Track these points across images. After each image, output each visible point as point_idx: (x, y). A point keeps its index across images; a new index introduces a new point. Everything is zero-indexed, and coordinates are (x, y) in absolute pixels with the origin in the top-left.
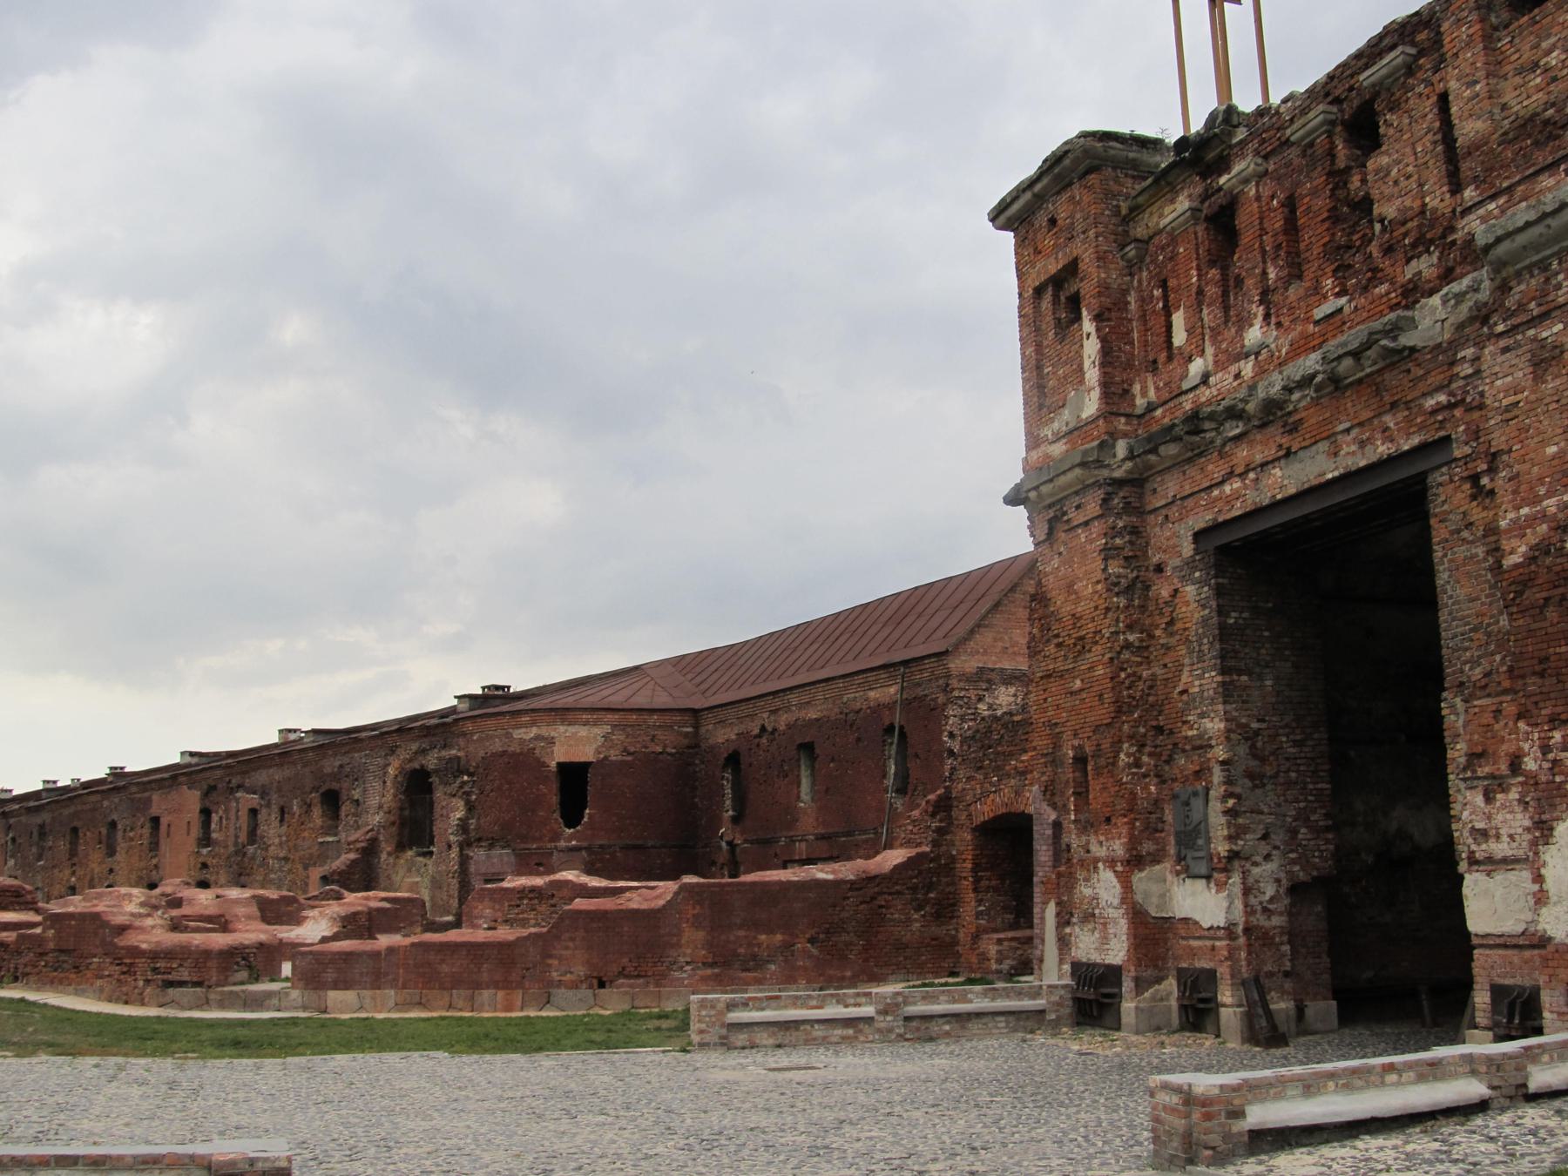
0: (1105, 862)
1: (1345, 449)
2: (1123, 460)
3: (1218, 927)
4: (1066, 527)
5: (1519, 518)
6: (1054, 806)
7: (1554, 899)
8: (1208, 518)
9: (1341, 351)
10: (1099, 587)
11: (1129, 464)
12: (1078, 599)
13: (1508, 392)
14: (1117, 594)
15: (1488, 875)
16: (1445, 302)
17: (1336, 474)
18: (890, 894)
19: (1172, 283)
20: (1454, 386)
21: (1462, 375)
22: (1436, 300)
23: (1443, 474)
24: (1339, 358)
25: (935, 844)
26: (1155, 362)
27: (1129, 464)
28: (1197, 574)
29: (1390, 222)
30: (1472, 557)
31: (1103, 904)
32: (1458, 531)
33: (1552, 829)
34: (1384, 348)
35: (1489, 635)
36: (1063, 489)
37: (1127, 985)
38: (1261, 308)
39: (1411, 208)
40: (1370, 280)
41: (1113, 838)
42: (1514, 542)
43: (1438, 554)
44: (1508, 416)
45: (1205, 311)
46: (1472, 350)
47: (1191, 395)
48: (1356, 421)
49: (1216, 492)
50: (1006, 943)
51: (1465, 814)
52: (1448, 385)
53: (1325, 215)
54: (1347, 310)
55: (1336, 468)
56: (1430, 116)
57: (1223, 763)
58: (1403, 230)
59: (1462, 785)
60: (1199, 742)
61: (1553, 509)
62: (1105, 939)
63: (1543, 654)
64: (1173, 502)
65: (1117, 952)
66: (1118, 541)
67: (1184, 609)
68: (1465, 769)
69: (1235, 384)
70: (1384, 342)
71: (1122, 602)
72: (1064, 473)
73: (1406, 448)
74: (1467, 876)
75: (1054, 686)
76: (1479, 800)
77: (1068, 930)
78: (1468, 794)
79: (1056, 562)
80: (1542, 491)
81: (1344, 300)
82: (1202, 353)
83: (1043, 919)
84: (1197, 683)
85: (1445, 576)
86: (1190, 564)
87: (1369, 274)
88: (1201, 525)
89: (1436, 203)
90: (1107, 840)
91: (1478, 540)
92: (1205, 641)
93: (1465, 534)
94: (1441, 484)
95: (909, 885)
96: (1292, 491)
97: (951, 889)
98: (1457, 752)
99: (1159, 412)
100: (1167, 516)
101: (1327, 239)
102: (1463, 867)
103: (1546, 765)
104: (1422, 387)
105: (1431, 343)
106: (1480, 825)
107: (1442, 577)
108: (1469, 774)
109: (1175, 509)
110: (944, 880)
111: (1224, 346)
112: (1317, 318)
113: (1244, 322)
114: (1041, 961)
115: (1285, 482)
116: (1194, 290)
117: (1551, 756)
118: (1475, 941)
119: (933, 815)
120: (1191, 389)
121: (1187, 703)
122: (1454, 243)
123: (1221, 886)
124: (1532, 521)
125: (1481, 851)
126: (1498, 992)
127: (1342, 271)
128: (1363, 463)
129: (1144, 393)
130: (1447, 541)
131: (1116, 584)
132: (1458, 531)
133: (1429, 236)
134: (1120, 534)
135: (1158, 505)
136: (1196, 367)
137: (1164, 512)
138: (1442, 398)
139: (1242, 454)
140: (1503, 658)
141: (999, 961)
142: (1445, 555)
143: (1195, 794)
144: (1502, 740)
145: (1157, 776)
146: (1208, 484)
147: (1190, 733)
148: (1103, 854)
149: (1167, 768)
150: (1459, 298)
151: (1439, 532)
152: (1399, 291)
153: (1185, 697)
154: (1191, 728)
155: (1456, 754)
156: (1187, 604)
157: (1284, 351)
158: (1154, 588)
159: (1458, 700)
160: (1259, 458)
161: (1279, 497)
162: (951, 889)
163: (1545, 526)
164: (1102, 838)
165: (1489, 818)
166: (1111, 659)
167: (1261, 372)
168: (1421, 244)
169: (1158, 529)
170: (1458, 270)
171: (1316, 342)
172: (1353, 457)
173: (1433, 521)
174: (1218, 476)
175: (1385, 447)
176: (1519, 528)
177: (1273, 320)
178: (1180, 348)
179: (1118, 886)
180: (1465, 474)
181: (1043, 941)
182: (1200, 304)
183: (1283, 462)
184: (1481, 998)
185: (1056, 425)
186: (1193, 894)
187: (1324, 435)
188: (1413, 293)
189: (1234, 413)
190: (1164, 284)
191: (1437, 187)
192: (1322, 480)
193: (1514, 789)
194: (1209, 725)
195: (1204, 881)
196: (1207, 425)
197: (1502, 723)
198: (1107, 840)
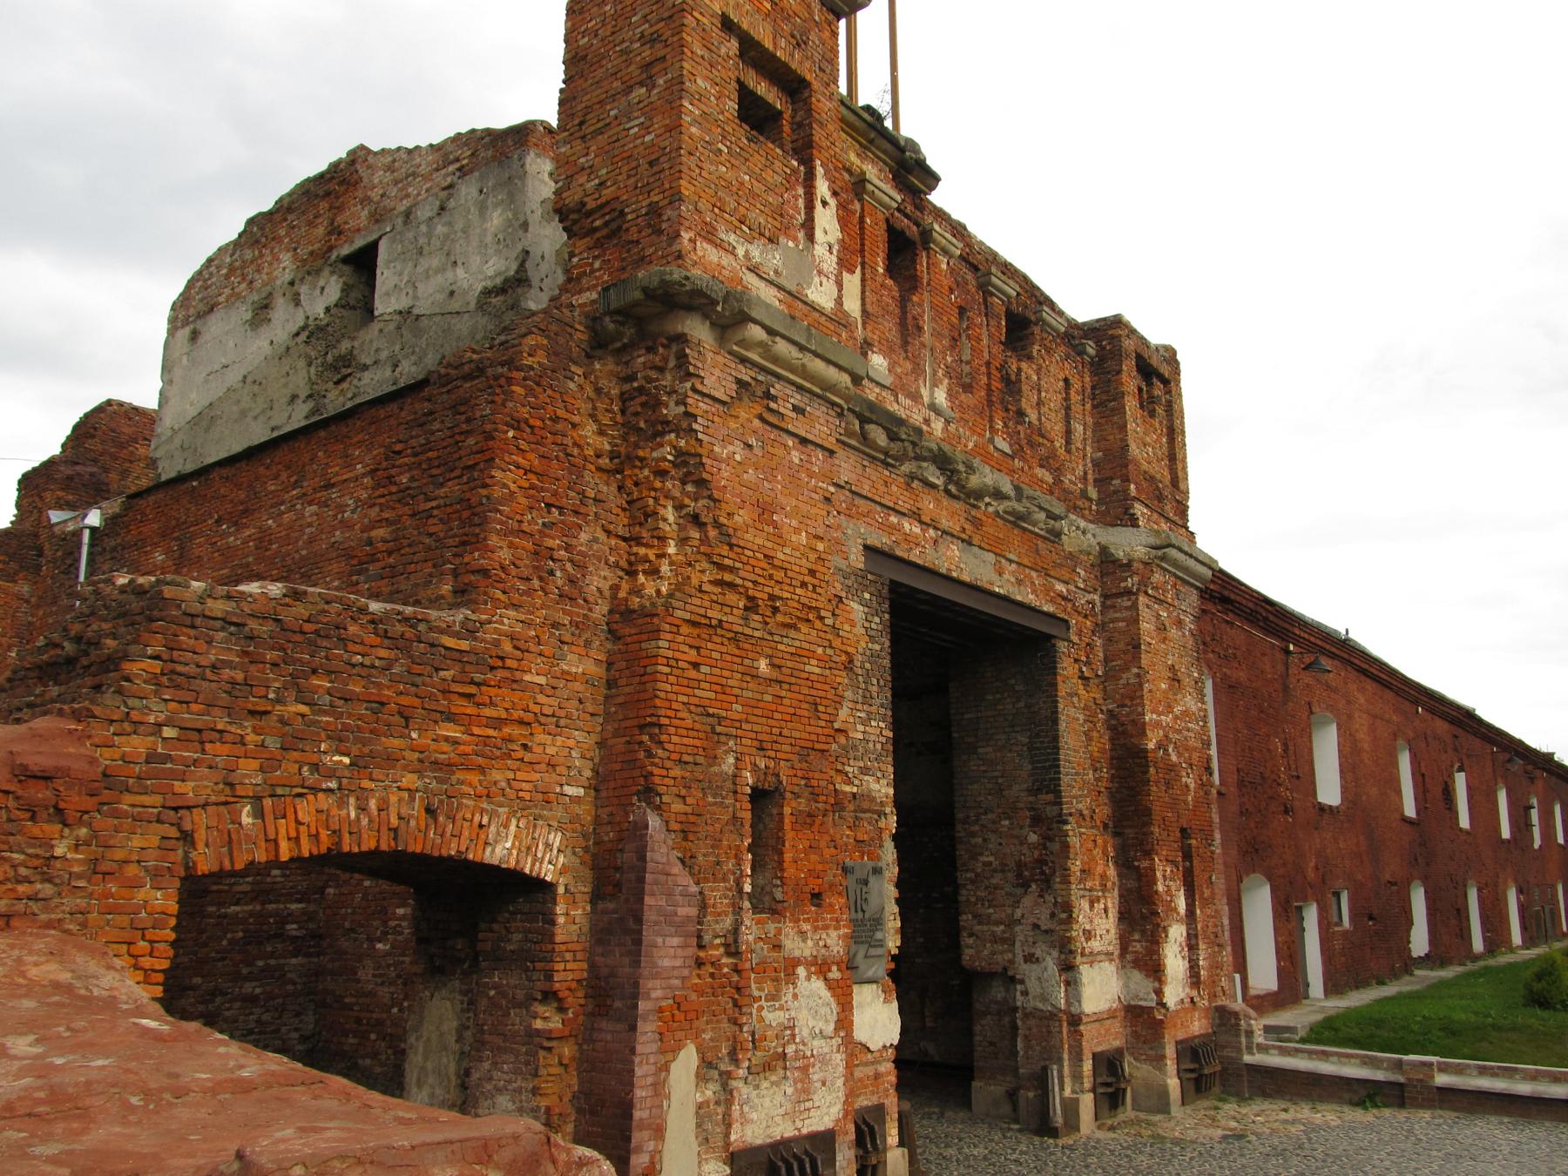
0: (808, 964)
4: (771, 419)
7: (1169, 980)
12: (779, 538)
17: (1002, 591)
31: (803, 1032)
36: (803, 372)
41: (826, 928)
47: (877, 390)
49: (894, 519)
58: (1041, 440)
60: (865, 805)
62: (804, 1093)
72: (829, 362)
73: (1045, 609)
83: (659, 1088)
88: (873, 541)
90: (816, 929)
92: (875, 682)
96: (966, 578)
98: (1076, 866)
106: (1088, 927)
107: (1062, 726)
111: (899, 370)
120: (878, 384)
126: (1095, 1056)
128: (1019, 598)
139: (928, 505)
146: (891, 505)
147: (847, 789)
148: (807, 953)
154: (850, 782)
156: (853, 624)
161: (954, 574)
164: (806, 927)
179: (834, 1006)
181: (659, 1132)
185: (756, 253)
187: (998, 551)
189: (942, 461)
192: (988, 587)
195: (874, 986)
198: (816, 929)
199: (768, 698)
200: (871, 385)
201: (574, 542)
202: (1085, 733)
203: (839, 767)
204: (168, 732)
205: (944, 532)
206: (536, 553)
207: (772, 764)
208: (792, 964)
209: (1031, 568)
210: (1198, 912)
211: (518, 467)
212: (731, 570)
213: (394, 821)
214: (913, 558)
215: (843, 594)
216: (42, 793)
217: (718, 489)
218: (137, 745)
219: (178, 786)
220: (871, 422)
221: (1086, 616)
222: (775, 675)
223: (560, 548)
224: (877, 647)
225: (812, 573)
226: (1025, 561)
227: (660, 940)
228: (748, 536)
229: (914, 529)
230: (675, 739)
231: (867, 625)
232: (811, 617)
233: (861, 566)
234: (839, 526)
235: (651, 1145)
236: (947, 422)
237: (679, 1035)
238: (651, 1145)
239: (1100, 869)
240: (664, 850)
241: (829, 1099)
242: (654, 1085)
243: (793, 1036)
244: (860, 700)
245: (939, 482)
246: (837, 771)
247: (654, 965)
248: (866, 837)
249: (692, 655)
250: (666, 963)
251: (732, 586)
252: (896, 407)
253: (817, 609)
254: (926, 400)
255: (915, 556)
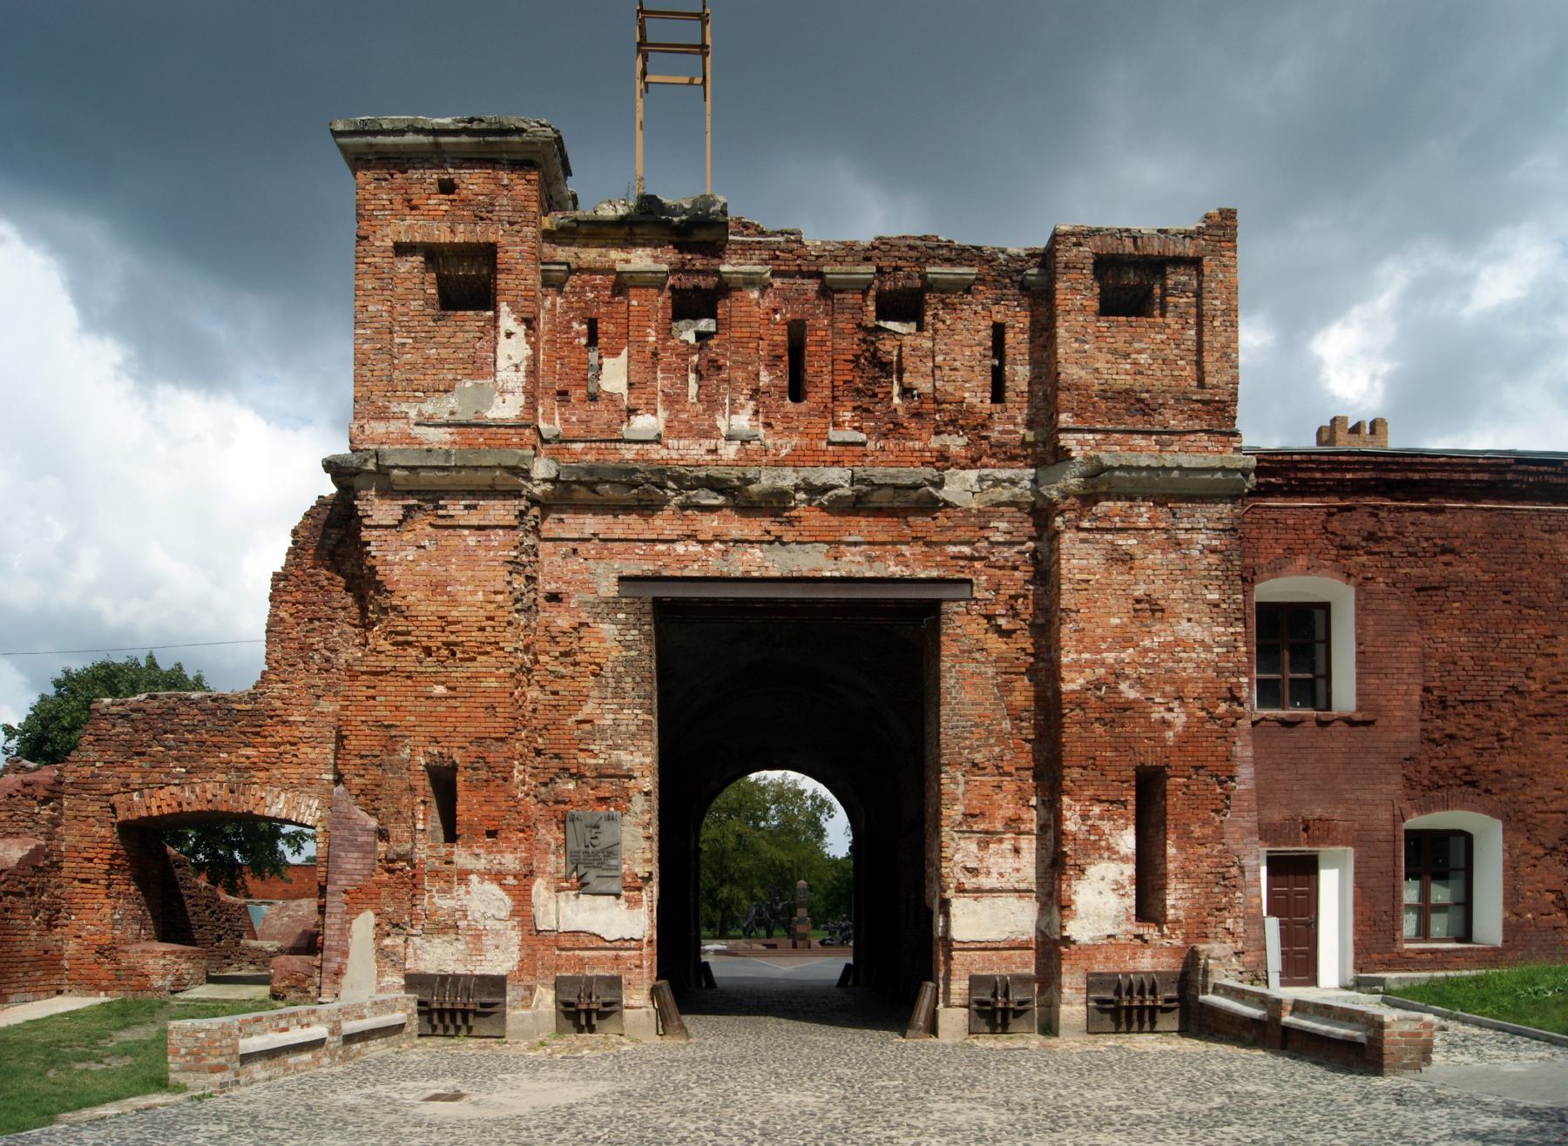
0: (480, 874)
1: (849, 557)
2: (545, 480)
3: (632, 939)
5: (1079, 660)
6: (374, 812)
8: (646, 567)
9: (889, 481)
10: (500, 598)
11: (549, 487)
13: (1081, 570)
14: (518, 611)
15: (976, 899)
16: (981, 479)
17: (836, 574)
18: (14, 894)
19: (603, 326)
20: (978, 545)
21: (992, 539)
22: (972, 475)
23: (959, 606)
24: (880, 486)
25: (50, 836)
26: (563, 394)
27: (549, 487)
28: (621, 616)
29: (919, 395)
30: (980, 674)
32: (970, 652)
33: (1083, 871)
34: (930, 493)
35: (990, 732)
37: (511, 995)
38: (752, 403)
39: (951, 394)
40: (890, 430)
42: (1074, 675)
43: (946, 664)
44: (1078, 587)
45: (659, 375)
46: (1006, 525)
47: (639, 446)
48: (871, 539)
49: (661, 547)
50: (168, 957)
51: (958, 857)
52: (974, 543)
53: (851, 358)
54: (871, 445)
55: (838, 570)
56: (982, 334)
57: (647, 794)
58: (936, 406)
59: (956, 836)
61: (1112, 661)
63: (1091, 755)
64: (588, 540)
65: (500, 961)
66: (524, 558)
67: (594, 644)
68: (960, 824)
69: (709, 458)
70: (931, 489)
71: (521, 619)
73: (922, 576)
74: (954, 901)
75: (389, 685)
76: (973, 847)
77: (387, 941)
78: (962, 843)
79: (411, 554)
80: (1104, 646)
81: (862, 437)
82: (655, 413)
83: (344, 932)
84: (612, 716)
85: (952, 682)
86: (613, 605)
87: (891, 426)
89: (976, 401)
91: (990, 662)
92: (629, 679)
93: (977, 655)
94: (957, 613)
95: (29, 885)
96: (775, 573)
97: (57, 892)
98: (953, 813)
99: (578, 446)
100: (575, 551)
101: (850, 378)
102: (949, 894)
103: (1084, 828)
104: (950, 535)
105: (965, 506)
107: (948, 682)
108: (964, 828)
109: (589, 545)
110: (53, 880)
111: (684, 416)
112: (833, 439)
113: (711, 404)
114: (339, 973)
115: (766, 564)
116: (649, 349)
117: (1089, 822)
118: (955, 945)
119: (46, 801)
120: (637, 442)
121: (589, 733)
122: (986, 438)
123: (633, 903)
124: (1092, 664)
125: (970, 882)
127: (863, 411)
129: (551, 421)
130: (957, 656)
131: (517, 601)
132: (970, 652)
133: (961, 422)
134: (525, 552)
135: (563, 536)
136: (645, 424)
137: (572, 545)
138: (966, 550)
139: (710, 524)
140: (1002, 750)
141: (163, 977)
142: (954, 667)
143: (610, 818)
144: (1000, 807)
145: (536, 797)
146: (655, 537)
147: (593, 761)
149: (543, 789)
150: (997, 482)
151: (948, 649)
152: (934, 454)
153: (587, 727)
154: (596, 756)
155: (953, 813)
156: (602, 640)
157: (783, 452)
158: (542, 614)
159: (959, 774)
160: (735, 533)
162: (57, 892)
163: (1102, 671)
165: (981, 860)
166: (512, 675)
167: (746, 459)
168: (953, 425)
169: (558, 559)
170: (985, 460)
171: (827, 459)
172: (853, 563)
173: (943, 638)
174: (668, 533)
175: (898, 568)
176: (1079, 667)
177: (761, 418)
178: (612, 394)
180: (984, 612)
181: (345, 954)
182: (655, 365)
183: (765, 546)
184: (959, 986)
186: (593, 909)
187: (827, 539)
188: (943, 459)
189: (714, 484)
190: (593, 325)
191: (981, 389)
192: (818, 575)
193: (1007, 842)
194: (624, 756)
195: (612, 898)
196: (670, 484)
197: (1001, 795)
198: (489, 853)
199: (443, 709)
200: (628, 446)
201: (329, 636)
202: (997, 686)
203: (582, 746)
204: (98, 764)
205: (736, 541)
206: (301, 648)
207: (445, 750)
208: (464, 875)
209: (894, 543)
210: (1171, 851)
211: (286, 602)
212: (408, 633)
213: (210, 797)
214: (686, 573)
215: (590, 620)
216: (28, 790)
217: (392, 583)
218: (87, 771)
219: (105, 786)
220: (597, 483)
221: (1015, 568)
222: (451, 693)
223: (319, 642)
224: (633, 653)
225: (491, 618)
226: (881, 537)
227: (343, 854)
228: (419, 608)
229: (691, 548)
230: (354, 742)
231: (622, 638)
232: (489, 649)
233: (616, 594)
234: (587, 569)
235: (339, 959)
236: (745, 442)
237: (360, 906)
238: (339, 959)
239: (1009, 810)
240: (346, 805)
241: (502, 957)
242: (340, 929)
243: (465, 916)
244: (609, 695)
245: (721, 500)
246: (581, 750)
247: (339, 867)
248: (607, 795)
249: (371, 692)
250: (349, 866)
251: (410, 644)
252: (664, 452)
253: (497, 643)
254: (724, 430)
255: (694, 570)
